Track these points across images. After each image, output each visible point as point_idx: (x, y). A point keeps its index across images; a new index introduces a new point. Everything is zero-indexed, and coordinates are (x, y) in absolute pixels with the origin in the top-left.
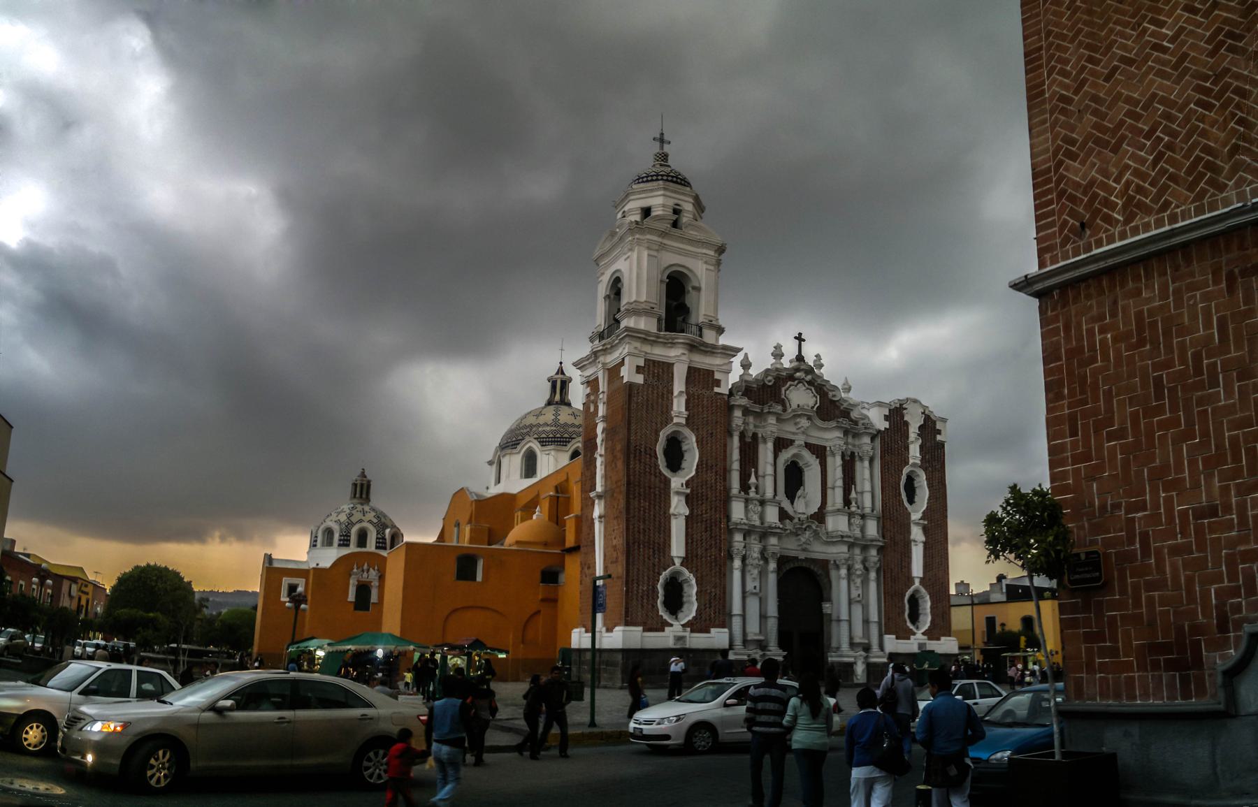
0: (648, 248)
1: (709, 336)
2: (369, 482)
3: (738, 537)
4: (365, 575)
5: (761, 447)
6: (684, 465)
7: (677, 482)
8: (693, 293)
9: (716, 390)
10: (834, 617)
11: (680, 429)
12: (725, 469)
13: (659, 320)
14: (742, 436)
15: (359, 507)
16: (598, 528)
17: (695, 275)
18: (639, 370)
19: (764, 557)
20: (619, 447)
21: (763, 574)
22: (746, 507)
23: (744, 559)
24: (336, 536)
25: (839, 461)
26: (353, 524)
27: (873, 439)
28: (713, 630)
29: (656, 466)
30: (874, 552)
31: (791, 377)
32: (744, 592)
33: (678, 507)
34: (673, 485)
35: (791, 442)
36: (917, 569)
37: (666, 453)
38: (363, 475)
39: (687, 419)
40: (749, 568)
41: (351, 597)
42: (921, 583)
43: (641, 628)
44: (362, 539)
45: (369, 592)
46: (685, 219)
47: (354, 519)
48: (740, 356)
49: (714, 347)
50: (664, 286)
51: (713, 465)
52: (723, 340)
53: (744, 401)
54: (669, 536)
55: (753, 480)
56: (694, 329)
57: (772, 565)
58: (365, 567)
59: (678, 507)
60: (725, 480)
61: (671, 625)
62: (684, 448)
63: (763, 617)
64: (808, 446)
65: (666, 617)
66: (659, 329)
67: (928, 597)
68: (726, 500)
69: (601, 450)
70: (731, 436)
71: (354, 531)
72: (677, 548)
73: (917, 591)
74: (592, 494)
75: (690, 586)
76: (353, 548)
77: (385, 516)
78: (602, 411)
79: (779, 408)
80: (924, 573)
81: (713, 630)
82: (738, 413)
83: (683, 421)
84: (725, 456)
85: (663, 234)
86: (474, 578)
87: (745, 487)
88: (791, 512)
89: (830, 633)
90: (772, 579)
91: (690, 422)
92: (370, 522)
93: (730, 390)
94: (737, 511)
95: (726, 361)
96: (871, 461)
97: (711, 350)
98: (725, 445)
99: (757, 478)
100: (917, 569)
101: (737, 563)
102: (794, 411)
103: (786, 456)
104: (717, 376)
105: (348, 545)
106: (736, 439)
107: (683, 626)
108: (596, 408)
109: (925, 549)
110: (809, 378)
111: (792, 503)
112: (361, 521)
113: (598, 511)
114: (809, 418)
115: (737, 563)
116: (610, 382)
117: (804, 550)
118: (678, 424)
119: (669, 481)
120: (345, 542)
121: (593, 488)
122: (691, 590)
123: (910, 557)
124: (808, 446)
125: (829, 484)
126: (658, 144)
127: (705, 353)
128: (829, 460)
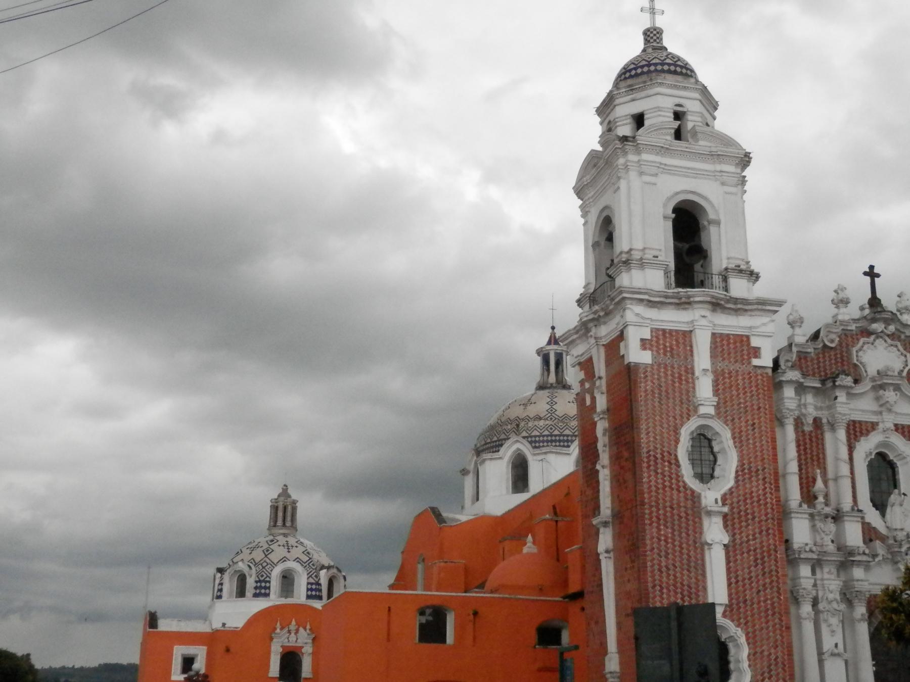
1: (739, 287)
2: (294, 502)
3: (805, 571)
4: (293, 637)
5: (828, 436)
7: (710, 496)
8: (713, 229)
9: (756, 362)
11: (709, 422)
12: (776, 473)
13: (666, 273)
14: (798, 423)
15: (282, 540)
16: (608, 568)
17: (713, 206)
18: (644, 344)
19: (848, 596)
21: (847, 623)
22: (813, 527)
23: (815, 602)
24: (251, 582)
26: (274, 565)
29: (679, 477)
32: (820, 653)
33: (715, 533)
34: (704, 502)
35: (873, 426)
39: (717, 407)
40: (822, 616)
45: (299, 663)
46: (690, 123)
47: (274, 557)
48: (784, 311)
49: (745, 301)
50: (670, 225)
51: (759, 470)
52: (759, 290)
53: (794, 375)
54: (704, 575)
55: (819, 484)
56: (717, 280)
57: (861, 610)
58: (293, 626)
59: (715, 533)
60: (777, 488)
66: (668, 286)
68: (783, 514)
69: (604, 458)
70: (782, 424)
71: (276, 574)
74: (595, 521)
75: (738, 646)
76: (274, 599)
78: (602, 403)
79: (848, 381)
82: (789, 392)
83: (711, 411)
84: (775, 455)
85: (663, 150)
86: (443, 639)
87: (809, 497)
88: (882, 529)
90: (863, 631)
91: (721, 410)
92: (297, 560)
93: (776, 362)
94: (801, 532)
95: (765, 319)
97: (739, 306)
98: (774, 440)
99: (825, 482)
101: (806, 609)
102: (873, 379)
103: (866, 447)
104: (755, 342)
105: (267, 595)
106: (790, 430)
108: (593, 399)
110: (892, 328)
111: (883, 515)
112: (284, 560)
113: (605, 540)
114: (897, 388)
115: (806, 609)
116: (608, 363)
119: (699, 496)
121: (596, 508)
126: (647, 16)
127: (737, 312)
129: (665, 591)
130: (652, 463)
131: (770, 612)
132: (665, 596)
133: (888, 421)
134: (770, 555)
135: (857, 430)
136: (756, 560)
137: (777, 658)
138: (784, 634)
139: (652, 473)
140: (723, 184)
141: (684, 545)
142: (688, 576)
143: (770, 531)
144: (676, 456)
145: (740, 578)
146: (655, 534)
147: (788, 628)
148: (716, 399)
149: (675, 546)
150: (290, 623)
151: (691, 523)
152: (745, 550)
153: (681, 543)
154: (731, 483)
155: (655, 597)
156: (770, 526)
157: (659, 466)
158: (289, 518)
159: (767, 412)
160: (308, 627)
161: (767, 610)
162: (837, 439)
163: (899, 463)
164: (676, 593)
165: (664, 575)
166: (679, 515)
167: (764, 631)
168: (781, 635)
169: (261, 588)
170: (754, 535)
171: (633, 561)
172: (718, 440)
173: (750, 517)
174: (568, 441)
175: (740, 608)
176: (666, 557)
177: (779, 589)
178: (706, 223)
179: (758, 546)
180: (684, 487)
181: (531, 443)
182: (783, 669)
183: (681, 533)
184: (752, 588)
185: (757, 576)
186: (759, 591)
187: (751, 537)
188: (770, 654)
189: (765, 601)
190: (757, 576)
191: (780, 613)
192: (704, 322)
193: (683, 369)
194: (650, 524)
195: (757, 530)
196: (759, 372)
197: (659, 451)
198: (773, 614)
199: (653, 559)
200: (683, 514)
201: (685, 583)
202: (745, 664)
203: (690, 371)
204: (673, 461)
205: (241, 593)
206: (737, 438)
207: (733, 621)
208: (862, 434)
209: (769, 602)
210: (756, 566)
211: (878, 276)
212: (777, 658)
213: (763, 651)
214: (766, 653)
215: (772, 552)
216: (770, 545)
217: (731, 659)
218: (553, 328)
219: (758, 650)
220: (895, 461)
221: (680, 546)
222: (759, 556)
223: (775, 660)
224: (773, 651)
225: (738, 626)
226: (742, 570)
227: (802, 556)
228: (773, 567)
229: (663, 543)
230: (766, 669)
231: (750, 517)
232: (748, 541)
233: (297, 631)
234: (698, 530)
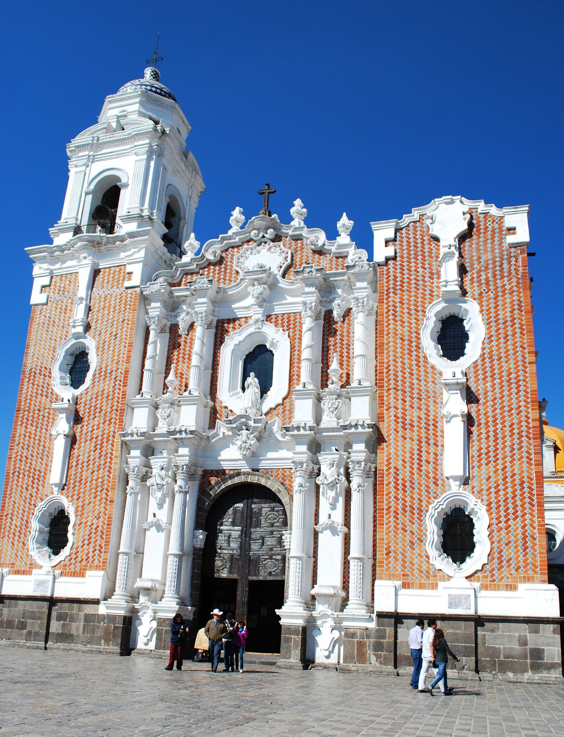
9: (127, 284)
61: (41, 567)
81: (88, 573)
104: (129, 269)
118: (77, 336)
129: (21, 476)
132: (20, 480)
134: (108, 441)
136: (95, 446)
137: (98, 527)
138: (108, 507)
139: (31, 385)
142: (41, 463)
143: (113, 420)
145: (80, 462)
146: (23, 432)
152: (89, 438)
153: (40, 437)
155: (13, 481)
156: (114, 416)
157: (37, 379)
159: (130, 323)
161: (97, 487)
164: (29, 477)
166: (43, 415)
167: (92, 505)
168: (105, 508)
170: (98, 425)
173: (98, 410)
175: (76, 486)
176: (27, 449)
177: (110, 468)
179: (100, 434)
180: (51, 393)
182: (101, 536)
183: (41, 428)
184: (89, 469)
185: (95, 459)
186: (94, 471)
188: (93, 524)
189: (96, 480)
190: (95, 459)
191: (107, 489)
193: (70, 301)
194: (21, 425)
197: (39, 368)
198: (101, 491)
199: (18, 451)
200: (46, 415)
204: (47, 374)
207: (68, 497)
208: (234, 328)
209: (100, 480)
210: (94, 451)
212: (98, 527)
213: (88, 521)
214: (89, 523)
215: (111, 438)
216: (110, 432)
219: (84, 521)
220: (272, 349)
222: (99, 442)
223: (96, 529)
225: (71, 501)
226: (83, 455)
228: (109, 451)
229: (27, 438)
230: (87, 537)
231: (98, 410)
232: (93, 430)
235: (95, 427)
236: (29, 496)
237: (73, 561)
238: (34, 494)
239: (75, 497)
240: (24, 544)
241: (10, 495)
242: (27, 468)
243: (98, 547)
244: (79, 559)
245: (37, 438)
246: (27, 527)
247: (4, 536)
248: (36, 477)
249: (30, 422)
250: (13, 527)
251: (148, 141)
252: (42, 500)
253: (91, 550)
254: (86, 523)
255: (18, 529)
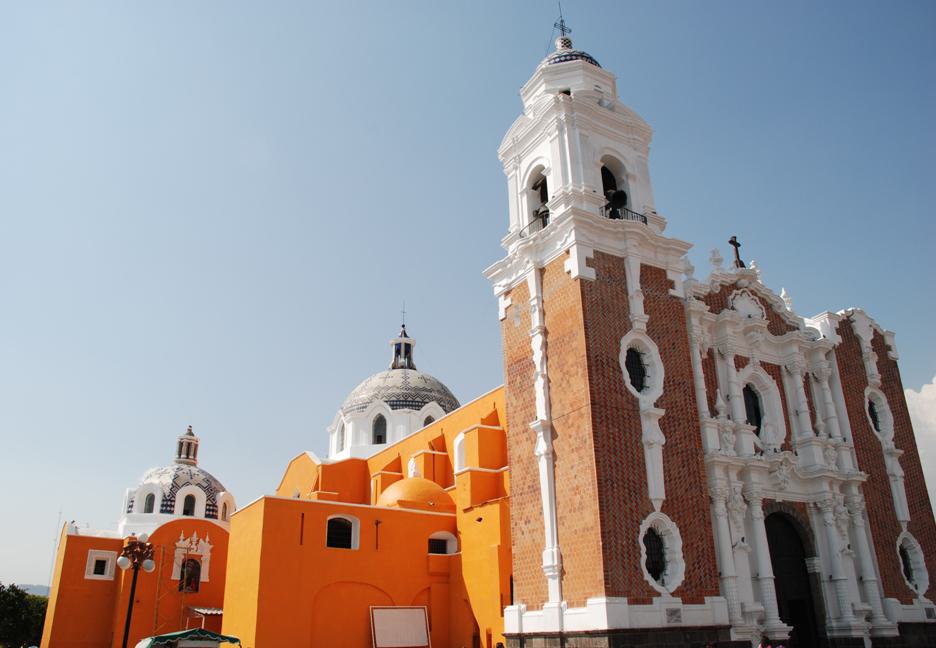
0: (580, 127)
6: (648, 382)
9: (672, 292)
10: (824, 577)
20: (571, 360)
21: (749, 521)
25: (800, 381)
27: (827, 355)
28: (707, 599)
29: (622, 382)
30: (855, 490)
31: (735, 286)
36: (903, 512)
37: (627, 364)
38: (190, 433)
41: (176, 575)
42: (910, 529)
43: (625, 600)
44: (190, 502)
52: (667, 234)
57: (759, 513)
58: (195, 537)
61: (659, 595)
62: (646, 360)
63: (756, 578)
64: (764, 365)
65: (652, 582)
67: (918, 547)
72: (656, 490)
73: (905, 539)
74: (533, 425)
77: (216, 481)
80: (911, 514)
81: (707, 599)
87: (714, 413)
88: (760, 446)
89: (821, 599)
96: (831, 381)
100: (903, 512)
104: (670, 276)
105: (171, 512)
107: (673, 594)
109: (906, 485)
112: (187, 484)
117: (781, 489)
120: (168, 507)
121: (533, 416)
122: (674, 545)
123: (891, 497)
124: (764, 365)
125: (791, 410)
128: (786, 381)
130: (600, 367)
131: (696, 509)
133: (757, 357)
135: (741, 362)
136: (683, 461)
140: (635, 149)
141: (628, 444)
144: (618, 363)
147: (710, 523)
148: (648, 317)
149: (621, 444)
150: (192, 535)
151: (632, 424)
154: (661, 392)
158: (192, 453)
160: (207, 539)
162: (727, 364)
163: (762, 393)
165: (614, 470)
169: (167, 506)
171: (581, 458)
172: (648, 354)
174: (418, 406)
178: (624, 178)
181: (390, 405)
187: (678, 441)
192: (634, 250)
195: (683, 436)
196: (674, 300)
200: (626, 416)
201: (631, 478)
202: (679, 555)
203: (625, 291)
204: (616, 367)
205: (149, 509)
206: (663, 353)
211: (739, 245)
214: (695, 545)
217: (667, 551)
218: (403, 326)
219: (689, 542)
221: (625, 445)
224: (700, 543)
227: (716, 459)
233: (198, 541)
234: (639, 432)
235: (678, 441)
236: (628, 511)
237: (688, 587)
238: (634, 509)
239: (676, 516)
240: (637, 569)
241: (607, 507)
242: (620, 477)
243: (707, 571)
244: (693, 584)
245: (622, 441)
246: (635, 548)
247: (612, 558)
248: (631, 488)
249: (610, 421)
250: (620, 547)
251: (555, 116)
252: (645, 517)
253: (702, 574)
254: (692, 544)
255: (626, 550)
